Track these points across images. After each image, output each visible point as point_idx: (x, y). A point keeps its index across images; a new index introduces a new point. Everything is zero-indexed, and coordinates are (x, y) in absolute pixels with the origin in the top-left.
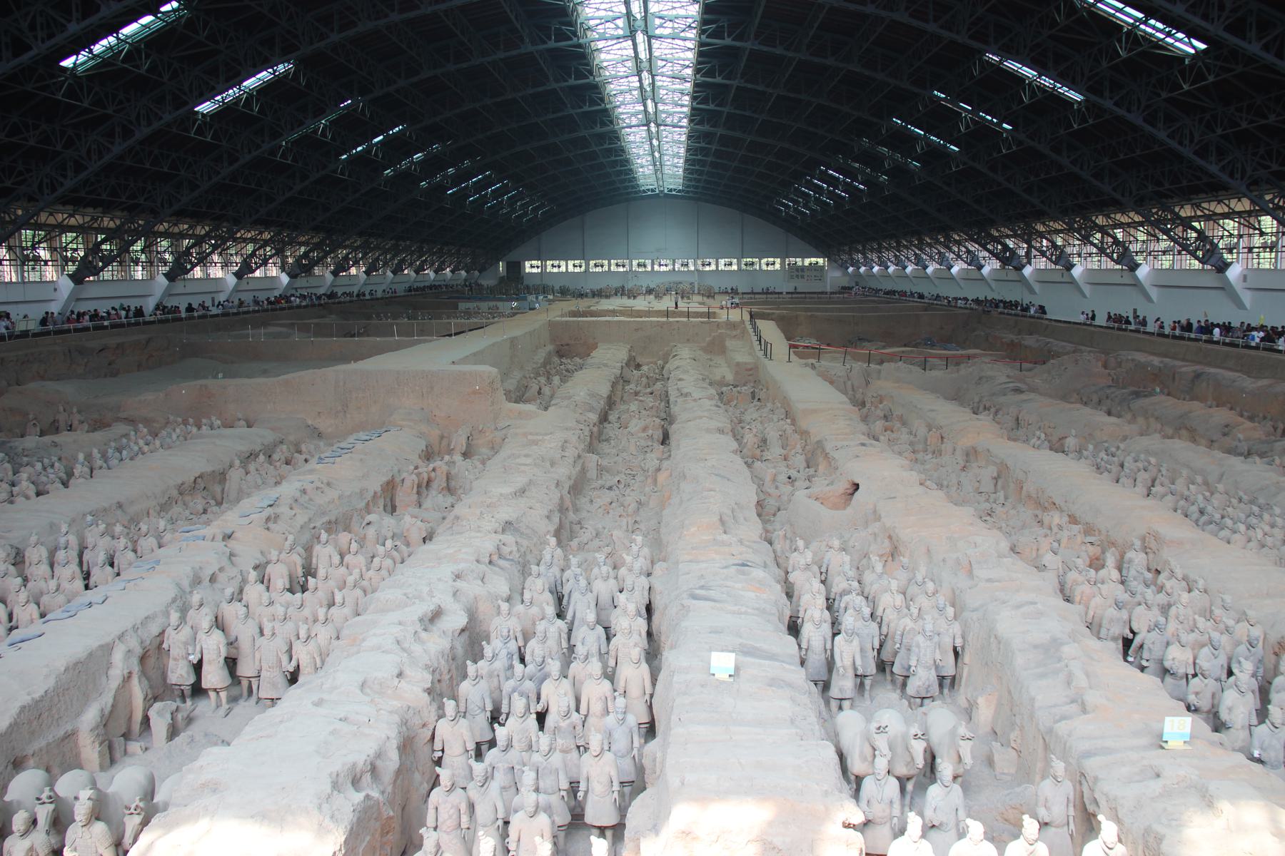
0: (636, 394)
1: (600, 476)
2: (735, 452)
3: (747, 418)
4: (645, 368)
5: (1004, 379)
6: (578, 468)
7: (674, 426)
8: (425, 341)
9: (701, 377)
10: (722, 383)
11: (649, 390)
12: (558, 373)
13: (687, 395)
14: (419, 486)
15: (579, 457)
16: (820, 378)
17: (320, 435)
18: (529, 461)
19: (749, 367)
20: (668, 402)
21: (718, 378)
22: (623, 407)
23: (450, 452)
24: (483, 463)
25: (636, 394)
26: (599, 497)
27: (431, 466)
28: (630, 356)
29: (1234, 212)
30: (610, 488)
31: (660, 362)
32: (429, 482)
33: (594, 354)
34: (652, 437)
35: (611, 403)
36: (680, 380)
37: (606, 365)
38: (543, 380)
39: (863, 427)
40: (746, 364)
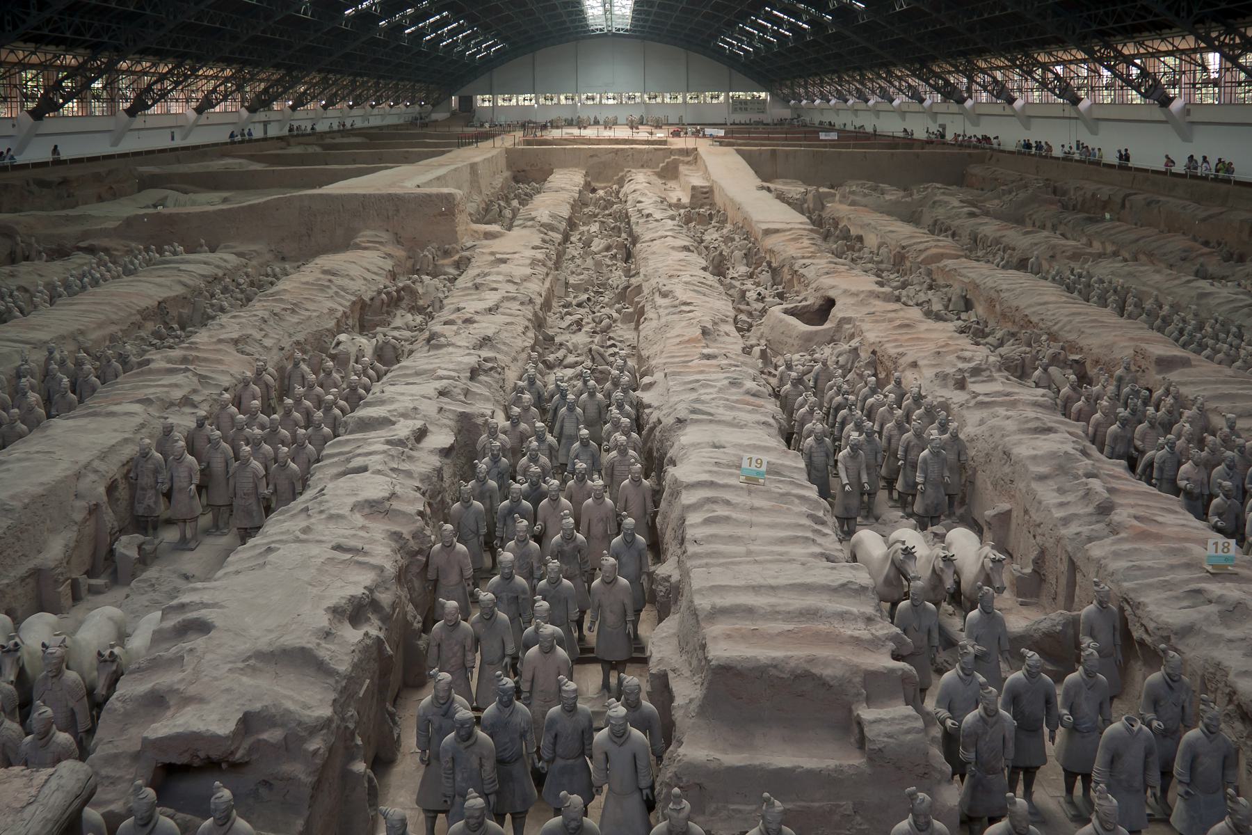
0: (596, 216)
3: (707, 237)
4: (601, 193)
5: (956, 203)
8: (387, 168)
9: (659, 200)
10: (678, 205)
11: (607, 212)
12: (516, 196)
13: (648, 215)
16: (778, 202)
19: (705, 190)
20: (628, 223)
21: (674, 201)
22: (582, 228)
25: (596, 216)
28: (586, 181)
31: (615, 187)
33: (551, 178)
35: (572, 224)
36: (639, 202)
37: (563, 189)
38: (502, 203)
40: (702, 187)
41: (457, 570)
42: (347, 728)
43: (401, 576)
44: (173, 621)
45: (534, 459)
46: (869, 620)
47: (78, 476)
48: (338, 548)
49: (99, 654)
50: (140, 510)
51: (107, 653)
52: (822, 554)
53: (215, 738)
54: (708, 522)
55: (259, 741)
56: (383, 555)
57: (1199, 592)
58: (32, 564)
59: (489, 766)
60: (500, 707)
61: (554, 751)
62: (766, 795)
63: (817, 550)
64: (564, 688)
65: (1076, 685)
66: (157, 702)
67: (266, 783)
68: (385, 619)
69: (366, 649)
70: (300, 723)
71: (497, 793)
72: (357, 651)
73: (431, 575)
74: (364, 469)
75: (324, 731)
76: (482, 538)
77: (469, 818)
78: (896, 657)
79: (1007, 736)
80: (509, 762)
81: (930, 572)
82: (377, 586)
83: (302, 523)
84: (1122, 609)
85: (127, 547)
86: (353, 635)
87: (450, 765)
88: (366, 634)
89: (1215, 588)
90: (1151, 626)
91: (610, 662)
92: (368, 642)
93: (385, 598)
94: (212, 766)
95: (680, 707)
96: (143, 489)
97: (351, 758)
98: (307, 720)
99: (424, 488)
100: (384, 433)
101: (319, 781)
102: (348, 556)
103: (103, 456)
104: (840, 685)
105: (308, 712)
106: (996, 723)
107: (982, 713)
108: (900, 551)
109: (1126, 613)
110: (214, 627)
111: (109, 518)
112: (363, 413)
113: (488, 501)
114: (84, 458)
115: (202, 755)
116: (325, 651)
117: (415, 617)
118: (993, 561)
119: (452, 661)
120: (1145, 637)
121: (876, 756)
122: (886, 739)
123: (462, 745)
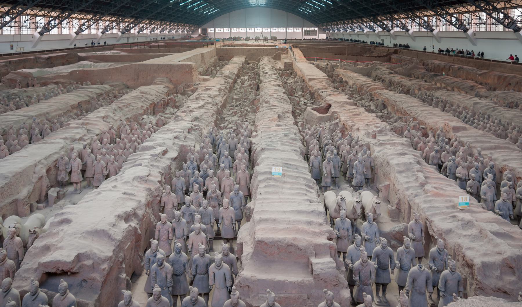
1: (232, 102)
2: (284, 93)
6: (224, 98)
7: (261, 84)
14: (164, 105)
15: (225, 95)
17: (128, 88)
18: (206, 96)
23: (177, 93)
24: (189, 97)
26: (232, 109)
27: (169, 98)
29: (469, 11)
30: (237, 106)
32: (168, 103)
34: (252, 88)
39: (332, 84)
41: (171, 203)
42: (119, 260)
43: (149, 204)
44: (58, 219)
45: (207, 163)
46: (321, 225)
47: (36, 165)
48: (125, 193)
49: (30, 231)
50: (59, 179)
51: (32, 231)
52: (308, 200)
53: (65, 263)
54: (266, 187)
55: (83, 264)
56: (142, 197)
57: (455, 216)
58: (14, 198)
59: (169, 276)
60: (176, 254)
61: (196, 271)
62: (268, 290)
63: (306, 198)
64: (200, 247)
65: (402, 251)
66: (47, 248)
67: (85, 280)
68: (141, 220)
69: (129, 231)
70: (99, 258)
71: (172, 287)
72: (125, 232)
73: (162, 205)
74: (140, 165)
75: (109, 261)
76: (184, 192)
77: (155, 295)
78: (330, 239)
79: (371, 271)
80: (178, 275)
81: (352, 207)
82: (137, 208)
83: (113, 184)
84: (426, 223)
85: (53, 192)
86: (124, 226)
87: (155, 275)
88: (130, 226)
89: (461, 215)
90: (435, 230)
91: (227, 239)
92: (130, 228)
93: (140, 213)
94: (64, 273)
95: (245, 256)
96: (61, 171)
97: (120, 273)
98: (102, 257)
99: (163, 172)
100: (152, 152)
101: (105, 280)
102: (127, 196)
103: (46, 159)
104: (305, 249)
105: (102, 254)
106: (367, 266)
107: (362, 262)
108: (340, 199)
109: (427, 224)
110: (72, 221)
111: (46, 182)
112: (145, 144)
113: (187, 178)
114: (38, 159)
115: (60, 269)
116: (111, 232)
117: (154, 220)
118: (376, 203)
119: (164, 236)
120: (433, 234)
121: (317, 277)
122: (320, 270)
123: (159, 268)
